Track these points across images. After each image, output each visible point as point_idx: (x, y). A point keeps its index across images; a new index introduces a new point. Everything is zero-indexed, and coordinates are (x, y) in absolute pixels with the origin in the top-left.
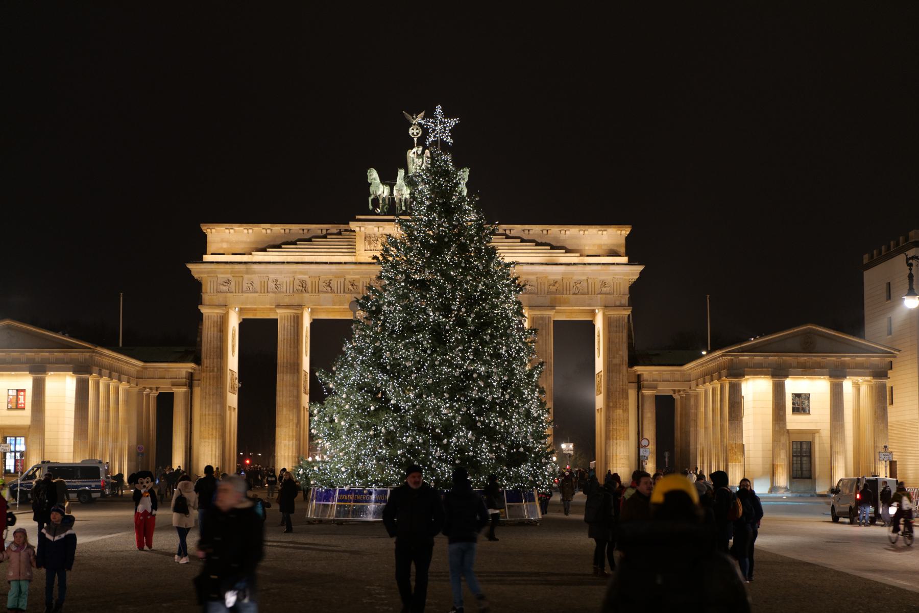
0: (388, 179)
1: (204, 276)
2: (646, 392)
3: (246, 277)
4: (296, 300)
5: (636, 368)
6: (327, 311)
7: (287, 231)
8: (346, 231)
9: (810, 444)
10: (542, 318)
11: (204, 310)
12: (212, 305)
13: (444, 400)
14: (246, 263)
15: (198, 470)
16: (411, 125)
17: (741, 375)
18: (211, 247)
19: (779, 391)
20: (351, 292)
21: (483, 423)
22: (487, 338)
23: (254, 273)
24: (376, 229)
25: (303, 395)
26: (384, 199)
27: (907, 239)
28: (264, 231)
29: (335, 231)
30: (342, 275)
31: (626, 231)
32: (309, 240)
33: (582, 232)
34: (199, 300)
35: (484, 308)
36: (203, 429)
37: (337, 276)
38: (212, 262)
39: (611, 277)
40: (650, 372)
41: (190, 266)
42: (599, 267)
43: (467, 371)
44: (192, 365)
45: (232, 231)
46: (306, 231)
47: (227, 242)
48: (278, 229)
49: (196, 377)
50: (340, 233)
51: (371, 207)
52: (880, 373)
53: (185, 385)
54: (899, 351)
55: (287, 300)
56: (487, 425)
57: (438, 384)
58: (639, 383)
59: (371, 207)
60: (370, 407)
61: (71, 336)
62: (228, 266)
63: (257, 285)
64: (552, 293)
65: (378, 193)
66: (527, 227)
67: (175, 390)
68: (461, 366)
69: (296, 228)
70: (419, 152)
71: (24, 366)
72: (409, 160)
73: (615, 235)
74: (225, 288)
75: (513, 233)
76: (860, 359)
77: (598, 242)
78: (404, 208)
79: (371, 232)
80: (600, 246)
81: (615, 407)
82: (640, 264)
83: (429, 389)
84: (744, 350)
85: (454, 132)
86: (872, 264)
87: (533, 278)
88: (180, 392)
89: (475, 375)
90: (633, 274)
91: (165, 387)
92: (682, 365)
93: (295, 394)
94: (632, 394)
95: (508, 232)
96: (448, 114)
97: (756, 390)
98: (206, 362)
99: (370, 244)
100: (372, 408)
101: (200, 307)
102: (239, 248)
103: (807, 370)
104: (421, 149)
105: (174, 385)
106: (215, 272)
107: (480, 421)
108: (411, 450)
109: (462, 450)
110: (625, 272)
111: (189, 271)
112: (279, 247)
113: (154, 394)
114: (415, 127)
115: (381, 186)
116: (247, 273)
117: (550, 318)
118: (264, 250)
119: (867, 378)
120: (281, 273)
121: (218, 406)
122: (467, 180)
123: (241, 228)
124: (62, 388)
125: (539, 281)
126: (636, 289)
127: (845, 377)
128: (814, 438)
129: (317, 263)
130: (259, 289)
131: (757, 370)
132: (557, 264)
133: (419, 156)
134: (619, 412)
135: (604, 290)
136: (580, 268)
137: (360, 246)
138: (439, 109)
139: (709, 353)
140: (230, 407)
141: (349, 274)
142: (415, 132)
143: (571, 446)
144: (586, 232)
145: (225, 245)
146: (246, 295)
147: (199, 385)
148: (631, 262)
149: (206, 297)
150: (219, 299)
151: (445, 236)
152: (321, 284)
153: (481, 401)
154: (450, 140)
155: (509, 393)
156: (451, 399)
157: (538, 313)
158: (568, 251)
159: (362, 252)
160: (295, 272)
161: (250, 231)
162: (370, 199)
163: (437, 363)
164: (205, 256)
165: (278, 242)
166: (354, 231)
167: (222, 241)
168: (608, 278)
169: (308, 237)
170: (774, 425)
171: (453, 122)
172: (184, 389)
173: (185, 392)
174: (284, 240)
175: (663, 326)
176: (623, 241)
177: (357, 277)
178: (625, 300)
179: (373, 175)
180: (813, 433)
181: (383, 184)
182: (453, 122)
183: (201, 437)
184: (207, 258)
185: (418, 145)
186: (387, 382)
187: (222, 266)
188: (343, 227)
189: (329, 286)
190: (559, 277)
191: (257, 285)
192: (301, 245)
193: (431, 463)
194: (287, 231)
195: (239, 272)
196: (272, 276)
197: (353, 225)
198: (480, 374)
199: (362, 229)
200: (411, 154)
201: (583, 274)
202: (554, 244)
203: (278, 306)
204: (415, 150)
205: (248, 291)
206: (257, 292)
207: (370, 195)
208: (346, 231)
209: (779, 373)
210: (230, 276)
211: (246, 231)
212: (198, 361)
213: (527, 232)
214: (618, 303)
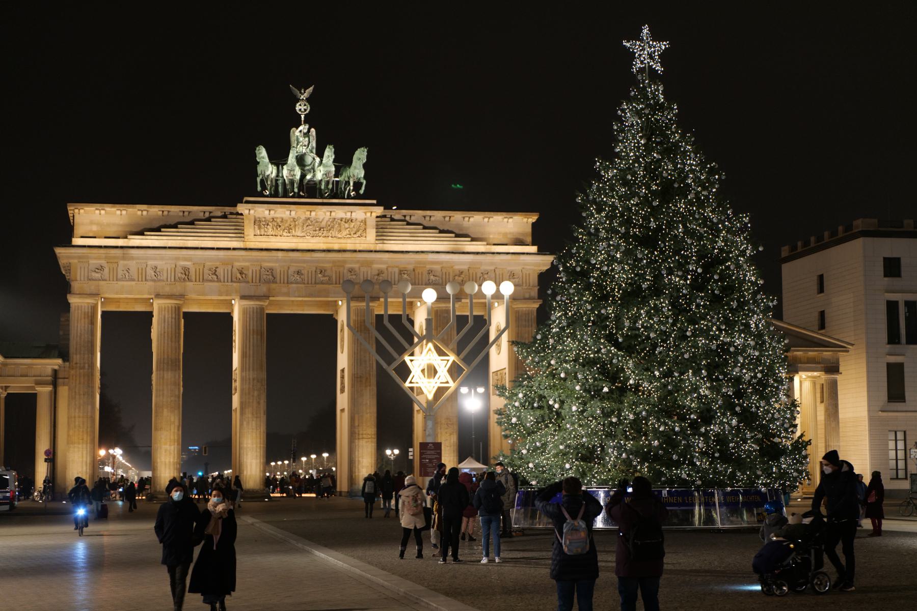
0: (278, 158)
1: (74, 261)
3: (121, 263)
4: (178, 289)
6: (198, 302)
7: (166, 213)
8: (232, 214)
11: (73, 300)
12: (82, 294)
13: (703, 378)
14: (122, 247)
15: (64, 478)
16: (298, 100)
18: (78, 230)
20: (239, 281)
21: (741, 405)
22: (734, 304)
23: (132, 258)
24: (267, 212)
27: (849, 228)
28: (140, 213)
29: (219, 214)
31: (533, 218)
32: (192, 223)
33: (486, 220)
35: (728, 268)
36: (71, 433)
37: (225, 262)
38: (84, 246)
39: (520, 268)
41: (59, 251)
42: (509, 257)
43: (724, 344)
44: (60, 361)
45: (103, 212)
46: (186, 214)
47: (98, 224)
48: (155, 211)
49: (60, 375)
50: (225, 216)
51: (259, 189)
52: (832, 368)
54: (852, 345)
55: (167, 290)
56: (745, 410)
57: (694, 358)
59: (259, 189)
60: (603, 387)
62: (102, 251)
63: (134, 272)
65: (268, 173)
66: (428, 213)
67: (39, 389)
68: (716, 338)
69: (175, 210)
70: (306, 131)
72: (293, 139)
73: (519, 223)
75: (413, 220)
76: (812, 353)
77: (503, 230)
78: (296, 190)
79: (261, 216)
80: (505, 234)
83: (683, 367)
85: (665, 57)
88: (44, 391)
89: (732, 349)
90: (544, 265)
91: (18, 386)
95: (408, 218)
96: (656, 36)
98: (75, 358)
99: (260, 228)
100: (606, 390)
101: (69, 296)
102: (111, 231)
104: (307, 126)
105: (39, 383)
107: (739, 405)
108: (668, 439)
109: (721, 440)
112: (158, 230)
113: (4, 395)
114: (302, 103)
115: (270, 165)
116: (124, 258)
117: (448, 311)
118: (141, 233)
119: (815, 374)
120: (162, 259)
121: (90, 407)
122: (365, 161)
125: (444, 271)
127: (797, 372)
129: (202, 248)
132: (464, 253)
133: (307, 134)
136: (489, 257)
138: (646, 30)
141: (238, 261)
142: (303, 108)
143: (396, 452)
144: (491, 220)
145: (94, 228)
146: (120, 283)
147: (64, 384)
148: (541, 252)
149: (75, 286)
150: (91, 287)
151: (674, 181)
152: (206, 271)
153: (738, 380)
154: (658, 68)
155: (762, 372)
156: (709, 377)
158: (473, 240)
159: (252, 237)
160: (177, 259)
161: (124, 212)
162: (259, 180)
163: (688, 334)
164: (74, 240)
165: (156, 225)
166: (242, 214)
167: (92, 223)
169: (188, 220)
171: (664, 45)
172: (49, 388)
173: (51, 392)
174: (148, 227)
176: (529, 229)
177: (247, 264)
178: (535, 292)
179: (262, 153)
181: (272, 163)
182: (664, 45)
183: (69, 442)
184: (77, 241)
185: (305, 122)
186: (623, 356)
188: (228, 209)
189: (215, 274)
190: (465, 267)
191: (134, 272)
192: (183, 229)
193: (692, 457)
194: (166, 213)
195: (114, 258)
196: (150, 263)
197: (241, 208)
198: (736, 347)
199: (252, 212)
200: (297, 133)
201: (492, 264)
202: (457, 232)
203: (158, 296)
204: (301, 128)
205: (124, 279)
206: (133, 280)
207: (257, 176)
208: (232, 214)
210: (103, 262)
211: (118, 212)
212: (65, 356)
213: (428, 218)
214: (527, 296)
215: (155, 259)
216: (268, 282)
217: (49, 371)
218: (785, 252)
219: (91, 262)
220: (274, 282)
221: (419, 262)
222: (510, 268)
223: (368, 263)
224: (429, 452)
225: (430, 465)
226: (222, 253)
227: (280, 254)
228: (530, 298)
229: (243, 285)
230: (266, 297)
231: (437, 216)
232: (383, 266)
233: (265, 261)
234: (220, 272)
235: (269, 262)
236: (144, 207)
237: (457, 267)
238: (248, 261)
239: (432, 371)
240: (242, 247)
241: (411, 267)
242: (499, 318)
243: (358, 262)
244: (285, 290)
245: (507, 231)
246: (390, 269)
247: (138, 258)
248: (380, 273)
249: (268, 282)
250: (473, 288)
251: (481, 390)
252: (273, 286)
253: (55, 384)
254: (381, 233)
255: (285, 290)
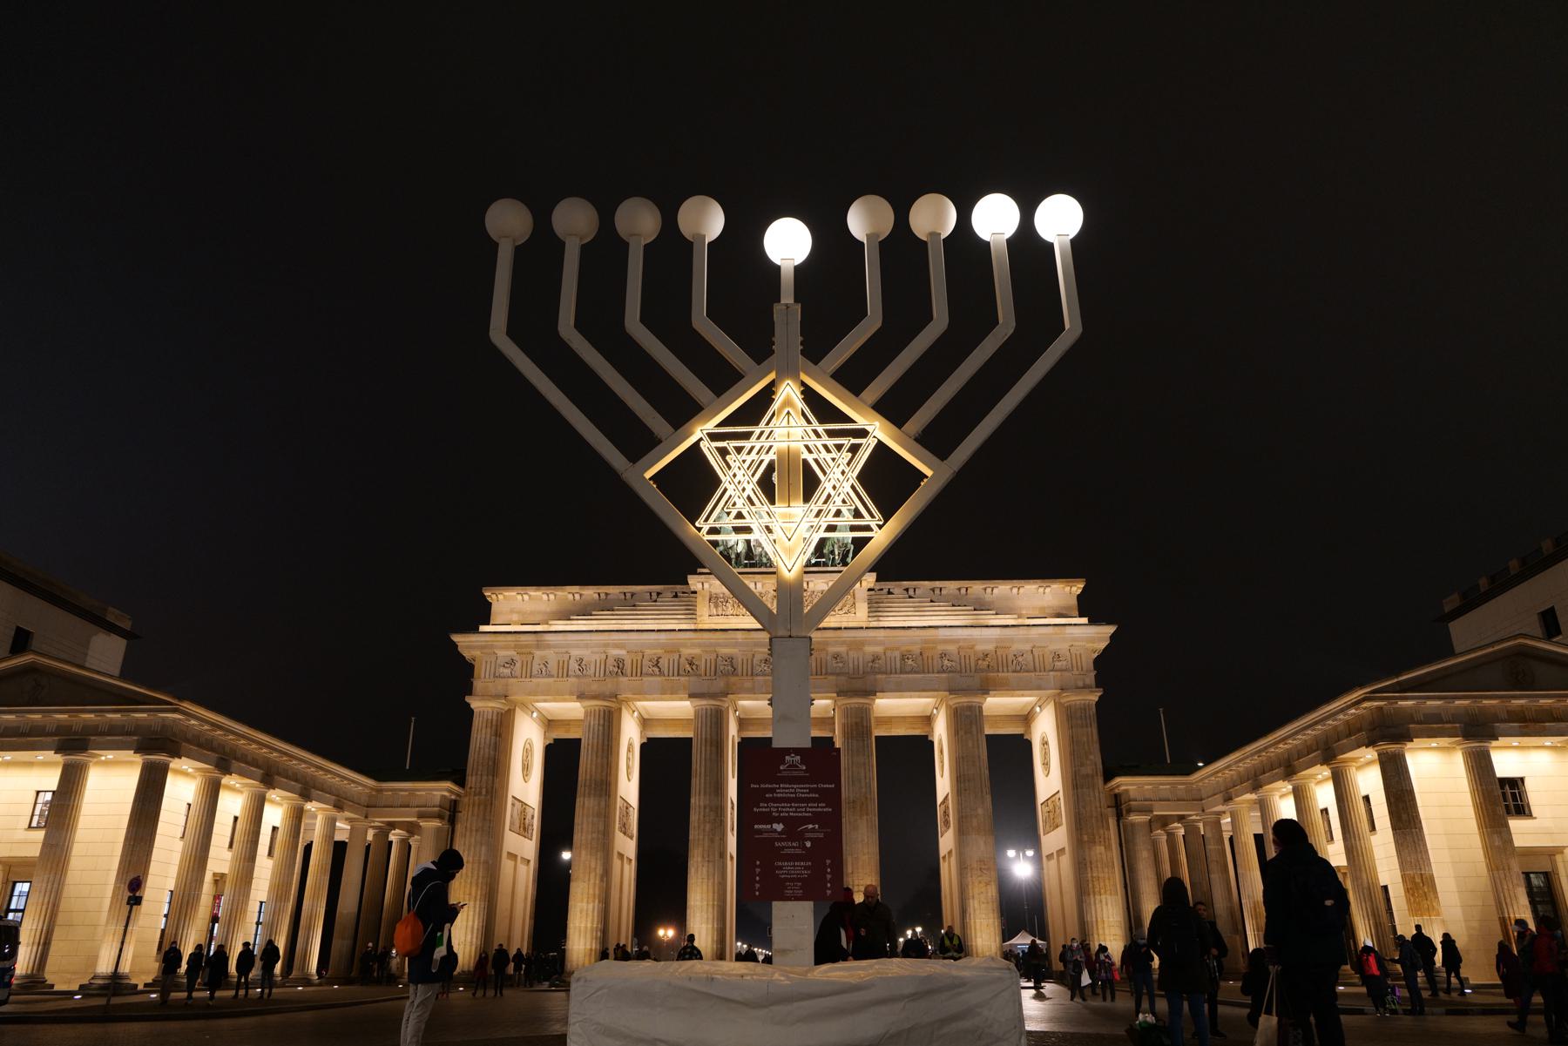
1: (477, 653)
2: (1135, 818)
3: (538, 653)
4: (608, 686)
5: (1118, 780)
9: (1549, 877)
10: (970, 708)
11: (475, 704)
17: (1406, 737)
19: (1480, 766)
23: (549, 647)
25: (619, 837)
26: (738, 555)
30: (672, 649)
31: (1077, 587)
34: (469, 690)
39: (1066, 646)
40: (1140, 786)
41: (456, 638)
44: (448, 785)
48: (590, 593)
53: (440, 817)
55: (595, 687)
58: (1119, 805)
61: (150, 688)
62: (509, 637)
63: (553, 666)
64: (982, 671)
66: (938, 584)
69: (614, 591)
71: (49, 739)
74: (507, 671)
80: (1042, 609)
81: (1093, 842)
82: (1109, 623)
84: (1404, 688)
86: (1471, 602)
87: (952, 648)
90: (1100, 640)
92: (1188, 774)
93: (601, 828)
94: (1112, 822)
97: (1436, 769)
98: (471, 780)
99: (716, 606)
101: (468, 699)
103: (1532, 725)
105: (421, 816)
106: (492, 647)
110: (1094, 637)
111: (455, 645)
116: (538, 647)
120: (587, 646)
123: (539, 593)
124: (111, 784)
126: (1105, 664)
128: (1554, 864)
130: (554, 672)
131: (1433, 726)
134: (1100, 849)
135: (1058, 664)
136: (1022, 631)
137: (703, 609)
139: (1207, 764)
140: (513, 856)
141: (685, 646)
145: (515, 617)
148: (1092, 622)
149: (478, 685)
150: (499, 686)
152: (645, 662)
157: (963, 700)
159: (706, 618)
160: (607, 645)
167: (512, 611)
168: (1062, 647)
170: (1482, 834)
172: (436, 823)
173: (438, 830)
175: (1147, 718)
176: (1074, 602)
177: (697, 651)
178: (1090, 678)
180: (1552, 853)
187: (501, 638)
188: (679, 588)
190: (990, 647)
191: (553, 666)
196: (575, 653)
201: (1027, 640)
209: (1476, 732)
210: (512, 653)
212: (461, 781)
214: (1080, 684)
215: (578, 647)
216: (725, 674)
217: (437, 801)
218: (1451, 602)
219: (501, 653)
220: (734, 672)
221: (926, 642)
222: (1054, 647)
223: (858, 645)
224: (784, 790)
225: (791, 847)
226: (663, 636)
227: (739, 635)
228: (1085, 687)
229: (693, 679)
230: (726, 694)
231: (951, 586)
232: (879, 649)
233: (719, 645)
234: (664, 663)
235: (726, 646)
236: (575, 589)
237: (979, 648)
238: (699, 645)
239: (792, 480)
240: (693, 627)
241: (916, 649)
242: (1045, 729)
243: (844, 643)
244: (748, 685)
245: (1045, 604)
246: (889, 653)
247: (555, 646)
248: (875, 658)
249: (725, 674)
250: (941, 216)
251: (1030, 853)
252: (733, 679)
253: (452, 821)
254: (875, 606)
255: (748, 685)
